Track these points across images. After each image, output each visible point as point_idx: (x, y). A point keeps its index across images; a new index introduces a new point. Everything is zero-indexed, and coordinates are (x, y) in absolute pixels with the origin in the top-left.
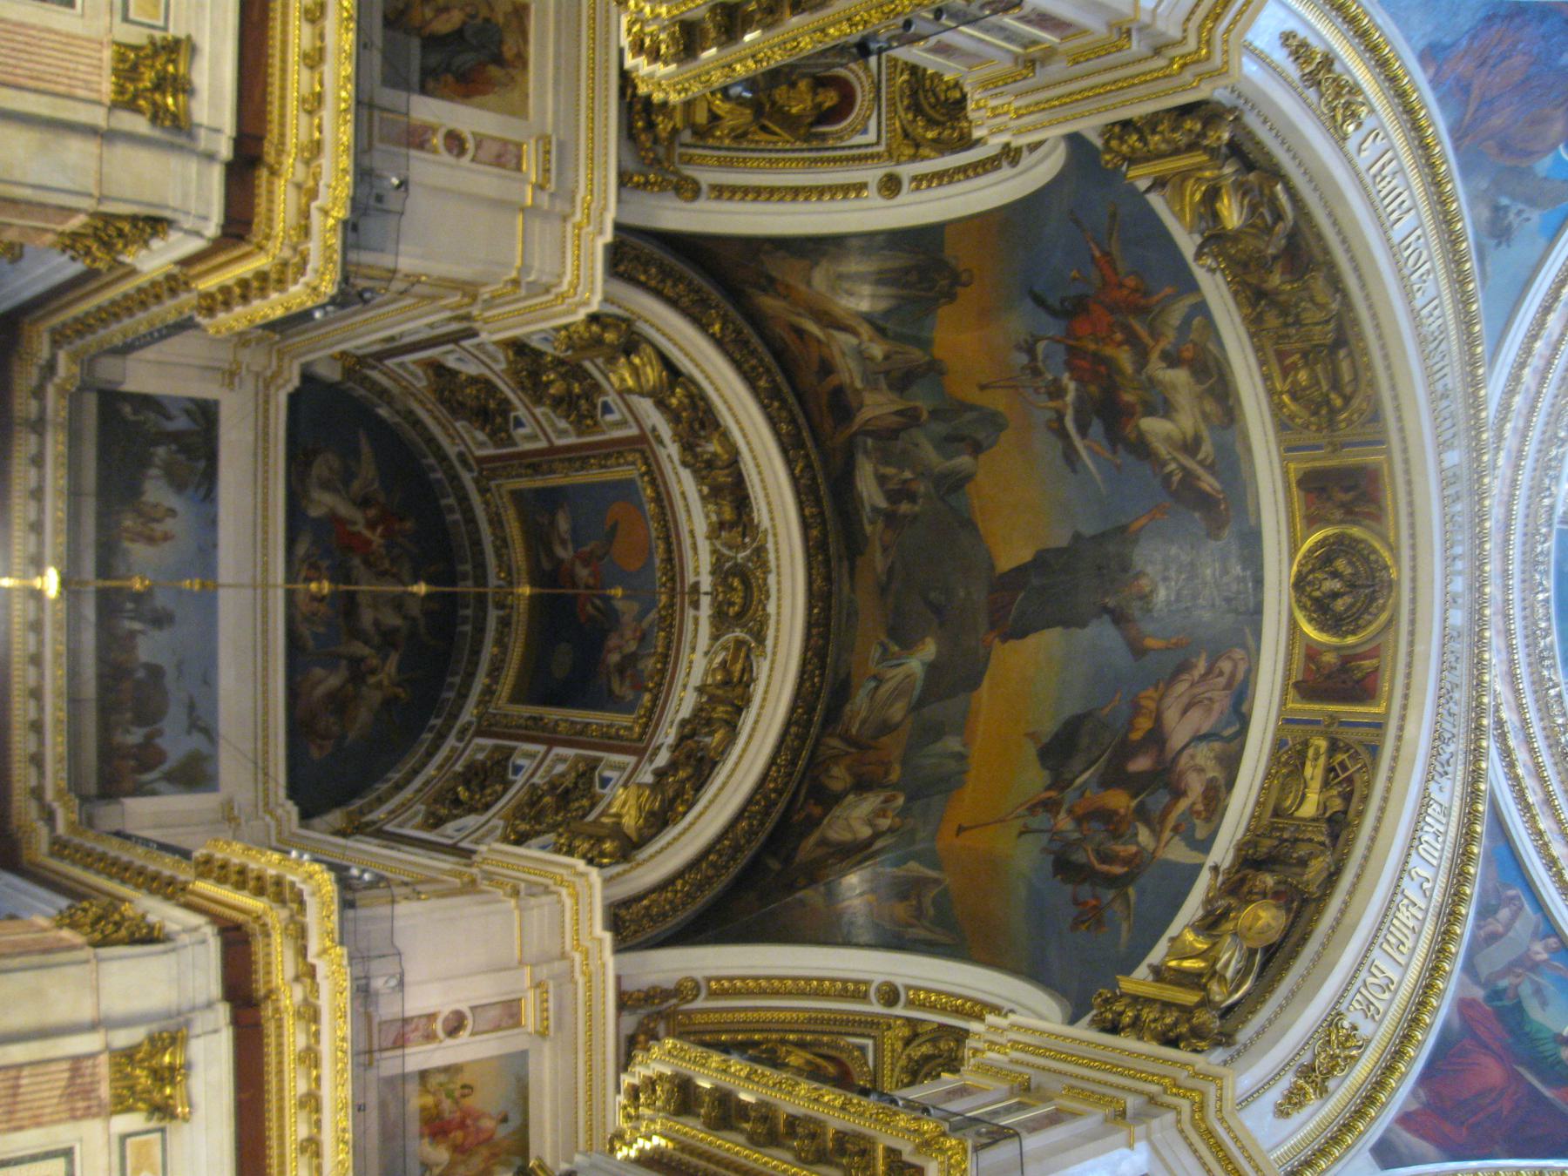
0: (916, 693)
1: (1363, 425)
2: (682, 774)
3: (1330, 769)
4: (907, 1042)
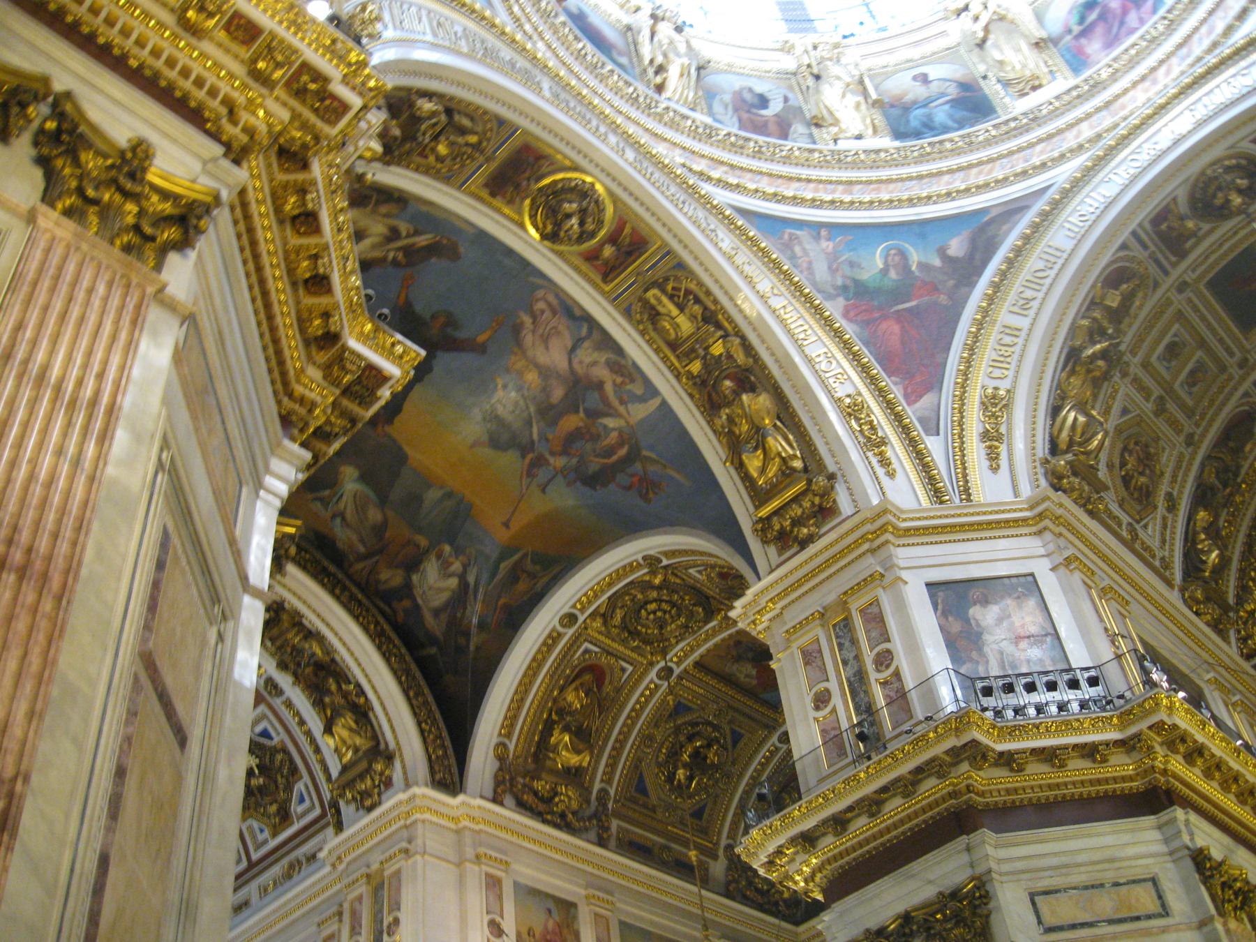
0: (372, 495)
1: (498, 133)
2: (334, 687)
3: (671, 297)
4: (605, 623)
